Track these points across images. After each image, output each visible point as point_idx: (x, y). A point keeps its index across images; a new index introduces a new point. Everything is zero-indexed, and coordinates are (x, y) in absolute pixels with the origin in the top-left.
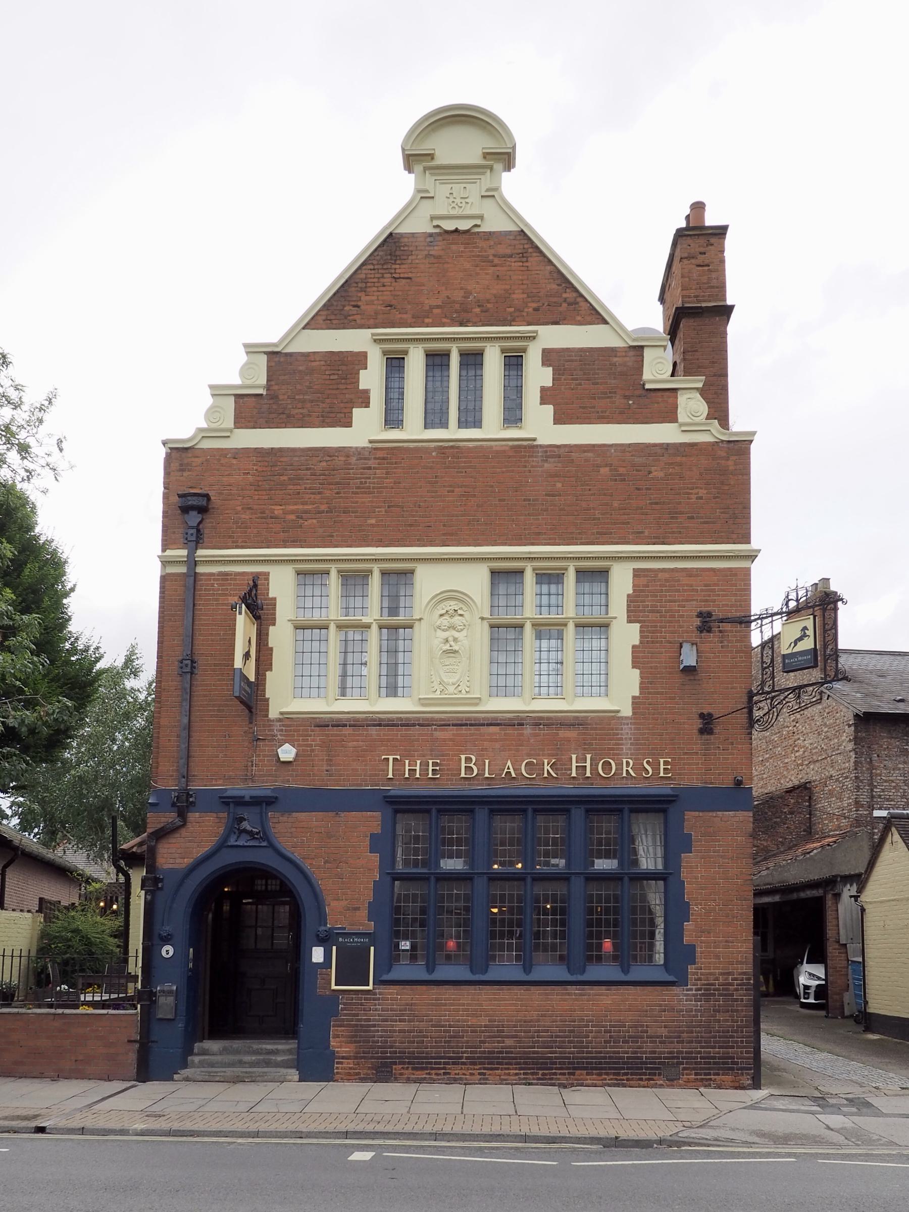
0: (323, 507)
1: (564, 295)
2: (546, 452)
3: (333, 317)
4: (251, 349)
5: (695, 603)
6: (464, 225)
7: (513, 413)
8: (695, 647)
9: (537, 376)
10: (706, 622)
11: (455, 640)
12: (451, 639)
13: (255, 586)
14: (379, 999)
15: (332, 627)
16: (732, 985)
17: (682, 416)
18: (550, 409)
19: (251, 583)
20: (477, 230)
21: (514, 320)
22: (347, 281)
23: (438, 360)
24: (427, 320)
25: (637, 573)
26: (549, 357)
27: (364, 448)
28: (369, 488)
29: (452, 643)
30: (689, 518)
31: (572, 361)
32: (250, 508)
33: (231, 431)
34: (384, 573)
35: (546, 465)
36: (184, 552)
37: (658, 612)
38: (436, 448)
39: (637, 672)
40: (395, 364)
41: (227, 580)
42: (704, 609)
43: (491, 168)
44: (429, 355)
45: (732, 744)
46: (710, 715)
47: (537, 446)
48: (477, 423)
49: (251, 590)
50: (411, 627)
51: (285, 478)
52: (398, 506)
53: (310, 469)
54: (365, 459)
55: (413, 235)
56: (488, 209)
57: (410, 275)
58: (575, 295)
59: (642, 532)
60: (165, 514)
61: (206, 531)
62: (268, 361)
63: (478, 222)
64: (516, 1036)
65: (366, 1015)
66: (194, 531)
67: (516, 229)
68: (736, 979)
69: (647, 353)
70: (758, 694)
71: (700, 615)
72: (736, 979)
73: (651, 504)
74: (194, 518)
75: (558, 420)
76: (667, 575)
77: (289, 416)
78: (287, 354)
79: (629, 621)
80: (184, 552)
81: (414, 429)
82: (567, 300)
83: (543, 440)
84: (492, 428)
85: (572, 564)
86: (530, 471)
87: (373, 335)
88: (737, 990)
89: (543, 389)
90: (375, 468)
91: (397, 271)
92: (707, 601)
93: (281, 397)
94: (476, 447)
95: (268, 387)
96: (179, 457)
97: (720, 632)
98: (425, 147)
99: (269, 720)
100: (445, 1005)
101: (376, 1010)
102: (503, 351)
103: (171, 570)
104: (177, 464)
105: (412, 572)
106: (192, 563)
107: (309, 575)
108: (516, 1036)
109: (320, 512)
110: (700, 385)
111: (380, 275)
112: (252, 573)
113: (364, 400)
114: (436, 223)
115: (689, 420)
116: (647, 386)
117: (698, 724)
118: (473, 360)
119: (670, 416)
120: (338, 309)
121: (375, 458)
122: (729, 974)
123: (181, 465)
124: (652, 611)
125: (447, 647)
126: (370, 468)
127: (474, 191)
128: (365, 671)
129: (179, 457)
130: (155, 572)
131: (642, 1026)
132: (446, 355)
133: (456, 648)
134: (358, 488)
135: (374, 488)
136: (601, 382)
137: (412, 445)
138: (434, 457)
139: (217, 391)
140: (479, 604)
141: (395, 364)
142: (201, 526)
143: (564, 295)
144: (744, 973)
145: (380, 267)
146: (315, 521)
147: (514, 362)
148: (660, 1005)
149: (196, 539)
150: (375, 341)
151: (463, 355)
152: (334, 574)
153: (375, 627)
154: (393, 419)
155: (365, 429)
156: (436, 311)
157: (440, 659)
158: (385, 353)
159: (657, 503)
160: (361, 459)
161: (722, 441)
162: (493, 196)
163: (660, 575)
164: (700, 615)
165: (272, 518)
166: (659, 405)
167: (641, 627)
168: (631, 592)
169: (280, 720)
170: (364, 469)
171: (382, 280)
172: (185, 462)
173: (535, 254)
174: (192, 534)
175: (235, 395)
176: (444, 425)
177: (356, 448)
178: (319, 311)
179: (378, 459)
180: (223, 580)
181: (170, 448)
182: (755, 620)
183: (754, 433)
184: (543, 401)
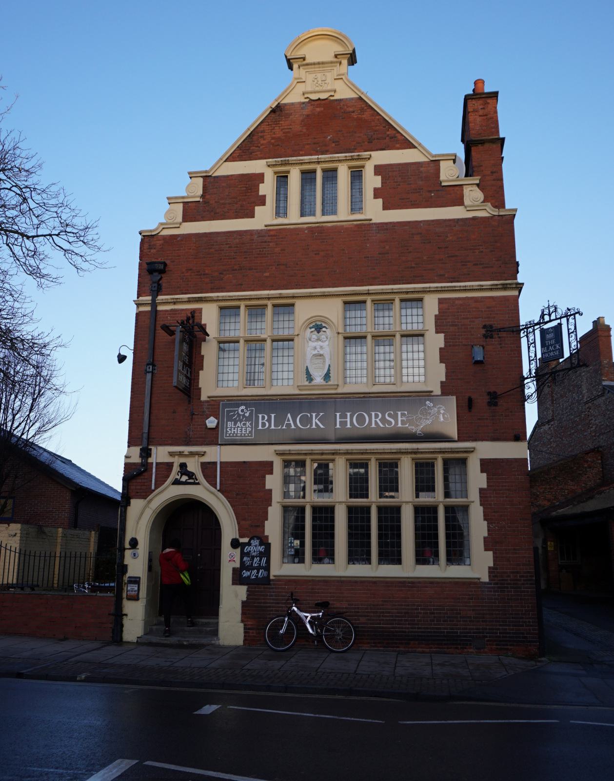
0: (236, 267)
1: (388, 133)
2: (378, 227)
3: (243, 154)
4: (192, 175)
5: (481, 319)
6: (323, 96)
7: (356, 205)
8: (481, 348)
9: (372, 181)
10: (490, 332)
11: (321, 347)
12: (318, 347)
13: (193, 317)
14: (273, 588)
15: (242, 341)
16: (520, 580)
17: (467, 201)
18: (380, 201)
19: (190, 315)
20: (332, 98)
21: (356, 149)
22: (252, 132)
23: (309, 176)
24: (301, 153)
25: (441, 301)
26: (379, 170)
27: (262, 230)
28: (265, 254)
29: (319, 350)
30: (474, 265)
31: (394, 171)
32: (191, 270)
33: (180, 224)
34: (274, 306)
35: (378, 235)
36: (150, 298)
37: (456, 325)
38: (308, 228)
39: (443, 365)
40: (282, 179)
41: (176, 314)
42: (487, 323)
43: (340, 63)
44: (303, 172)
45: (511, 412)
46: (495, 392)
47: (372, 224)
48: (334, 212)
49: (188, 319)
50: (292, 340)
51: (213, 250)
52: (283, 265)
53: (228, 244)
54: (262, 236)
55: (293, 104)
56: (339, 86)
57: (291, 127)
58: (394, 132)
59: (444, 275)
60: (140, 276)
61: (164, 285)
62: (203, 182)
63: (332, 94)
64: (368, 616)
65: (264, 599)
66: (156, 285)
67: (357, 96)
68: (523, 576)
69: (442, 163)
70: (527, 378)
71: (485, 327)
72: (523, 576)
73: (449, 257)
74: (156, 276)
75: (386, 207)
76: (461, 302)
77: (216, 213)
78: (215, 177)
79: (437, 332)
80: (150, 298)
81: (294, 217)
82: (391, 136)
83: (376, 220)
84: (343, 214)
85: (397, 297)
86: (368, 239)
87: (267, 162)
88: (523, 584)
89: (375, 190)
90: (269, 242)
91: (283, 125)
92: (489, 318)
93: (211, 202)
94: (332, 227)
95: (203, 196)
96: (148, 241)
97: (499, 337)
98: (300, 53)
99: (201, 402)
100: (318, 593)
101: (271, 596)
102: (350, 168)
103: (142, 309)
104: (147, 245)
105: (293, 305)
106: (154, 304)
107: (228, 311)
108: (368, 616)
109: (233, 270)
110: (478, 182)
111: (272, 128)
112: (191, 309)
113: (262, 201)
114: (306, 96)
115: (471, 204)
116: (443, 184)
117: (487, 399)
118: (331, 175)
119: (459, 201)
120: (246, 149)
121: (269, 236)
122: (517, 572)
123: (150, 246)
124: (453, 325)
125: (316, 352)
126: (265, 242)
127: (330, 76)
128: (263, 369)
129: (148, 241)
130: (133, 310)
131: (457, 610)
132: (314, 171)
133: (321, 352)
134: (258, 254)
135: (268, 254)
136: (414, 184)
137: (292, 227)
138: (306, 233)
139: (171, 201)
140: (336, 323)
141: (282, 179)
142: (161, 282)
143: (388, 133)
144: (529, 572)
145: (273, 123)
146: (231, 276)
147: (357, 175)
148: (469, 595)
149: (157, 290)
150: (269, 166)
151: (324, 171)
152: (242, 308)
153: (269, 341)
154: (281, 209)
155: (263, 218)
156: (307, 147)
157: (311, 360)
158: (275, 173)
159: (452, 256)
160: (260, 236)
161: (495, 215)
162: (342, 79)
163: (457, 302)
164: (485, 327)
165: (204, 275)
166: (452, 196)
167: (445, 336)
168: (437, 313)
169: (207, 402)
170: (262, 242)
171: (273, 131)
172: (152, 243)
173: (368, 110)
174: (155, 287)
175: (183, 202)
176: (313, 214)
177: (257, 230)
178: (235, 150)
179: (272, 236)
180: (173, 314)
181: (144, 236)
182: (523, 329)
183: (516, 210)
184: (376, 196)
